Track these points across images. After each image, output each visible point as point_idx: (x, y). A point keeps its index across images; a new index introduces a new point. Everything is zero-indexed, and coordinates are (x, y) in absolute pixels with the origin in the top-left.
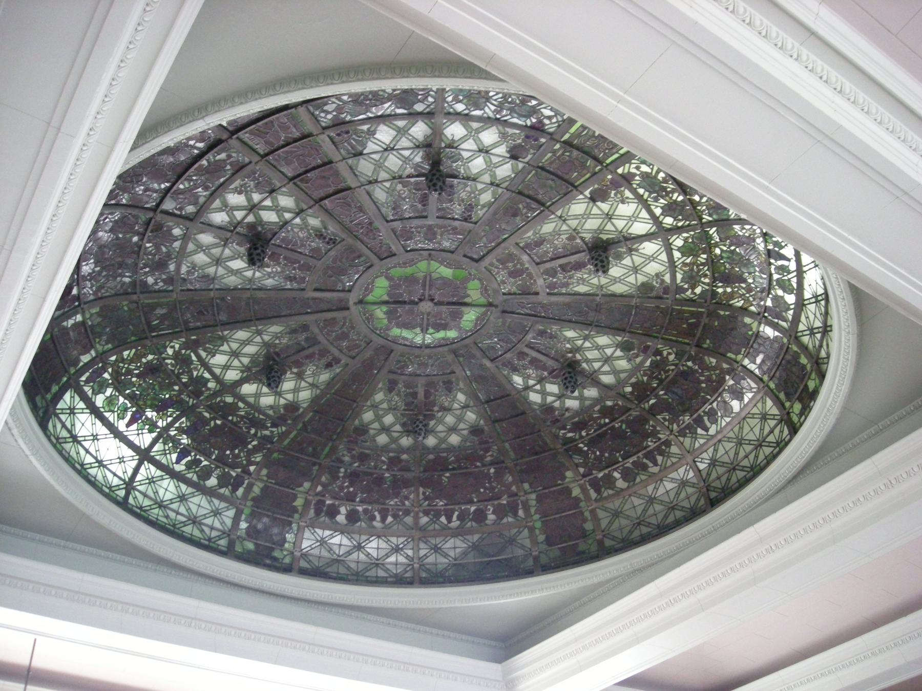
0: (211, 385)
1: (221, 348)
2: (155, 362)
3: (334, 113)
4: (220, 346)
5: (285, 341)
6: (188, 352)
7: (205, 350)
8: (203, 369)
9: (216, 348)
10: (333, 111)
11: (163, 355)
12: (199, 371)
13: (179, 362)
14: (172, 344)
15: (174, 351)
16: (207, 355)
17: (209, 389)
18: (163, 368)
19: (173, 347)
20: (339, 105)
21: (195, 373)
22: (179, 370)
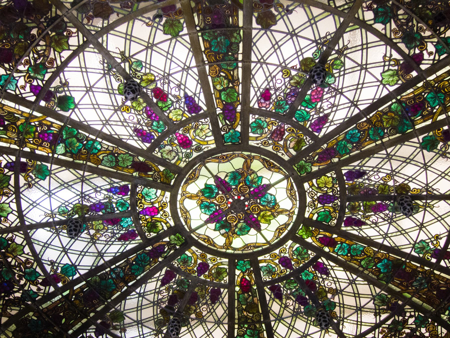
0: (369, 15)
1: (381, 70)
2: (442, 29)
3: (407, 318)
4: (384, 72)
5: (325, 105)
6: (412, 52)
7: (397, 61)
8: (388, 36)
9: (386, 68)
10: (408, 319)
11: (435, 40)
12: (391, 31)
13: (416, 35)
14: (432, 57)
15: (426, 49)
16: (391, 55)
17: (369, 8)
18: (430, 22)
19: (430, 54)
20: (407, 324)
21: (394, 26)
22: (413, 25)
